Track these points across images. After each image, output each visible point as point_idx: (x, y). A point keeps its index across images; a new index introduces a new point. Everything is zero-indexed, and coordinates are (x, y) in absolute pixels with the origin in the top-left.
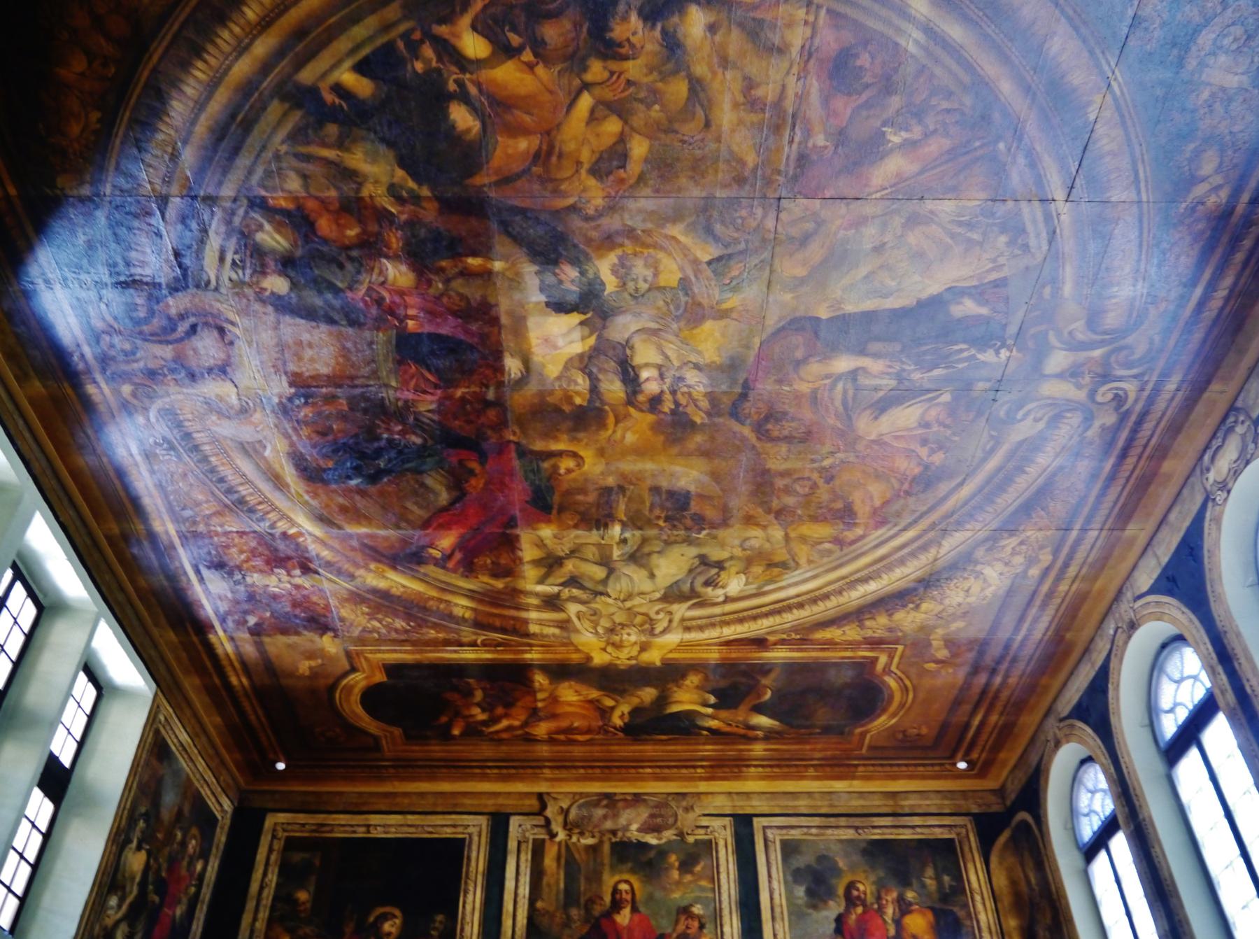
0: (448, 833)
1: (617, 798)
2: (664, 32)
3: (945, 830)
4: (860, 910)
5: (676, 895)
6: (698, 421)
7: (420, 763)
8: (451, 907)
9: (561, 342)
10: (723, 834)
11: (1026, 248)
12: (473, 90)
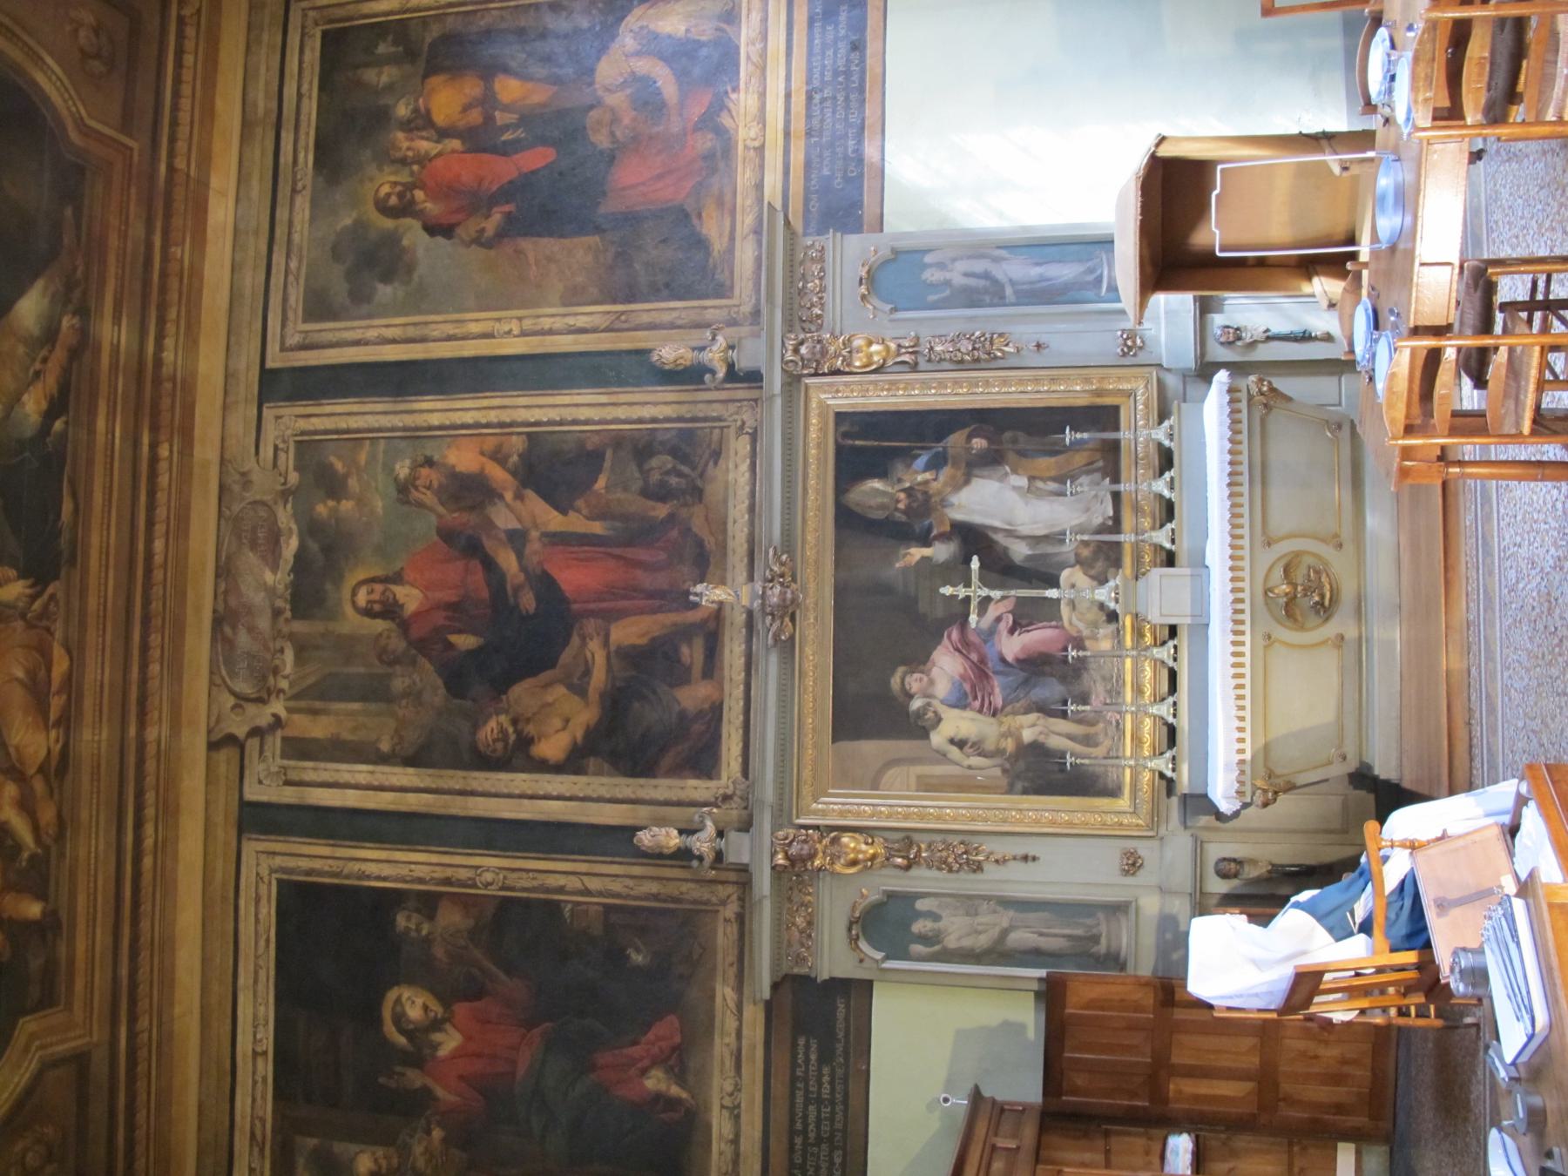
0: (269, 911)
1: (221, 608)
3: (308, 43)
4: (419, 194)
5: (379, 505)
7: (124, 972)
8: (385, 902)
10: (291, 420)
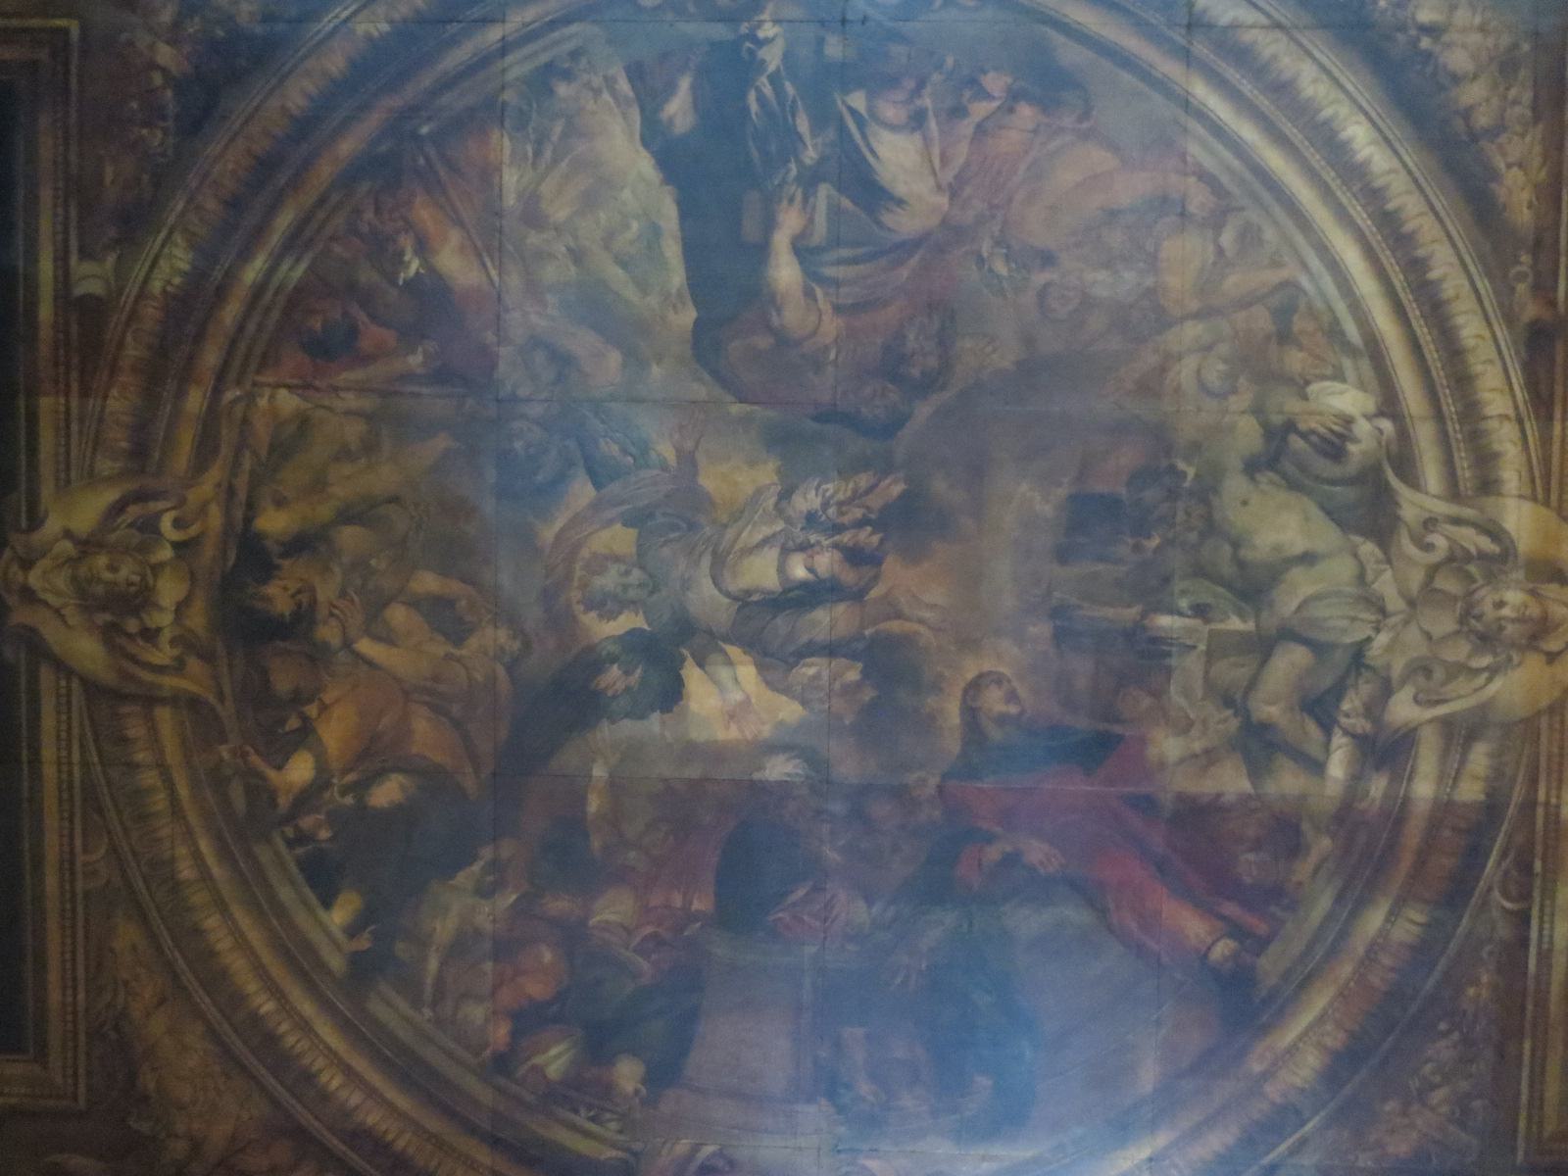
2: (286, 555)
6: (897, 489)
9: (737, 696)
11: (575, 55)
12: (351, 777)
